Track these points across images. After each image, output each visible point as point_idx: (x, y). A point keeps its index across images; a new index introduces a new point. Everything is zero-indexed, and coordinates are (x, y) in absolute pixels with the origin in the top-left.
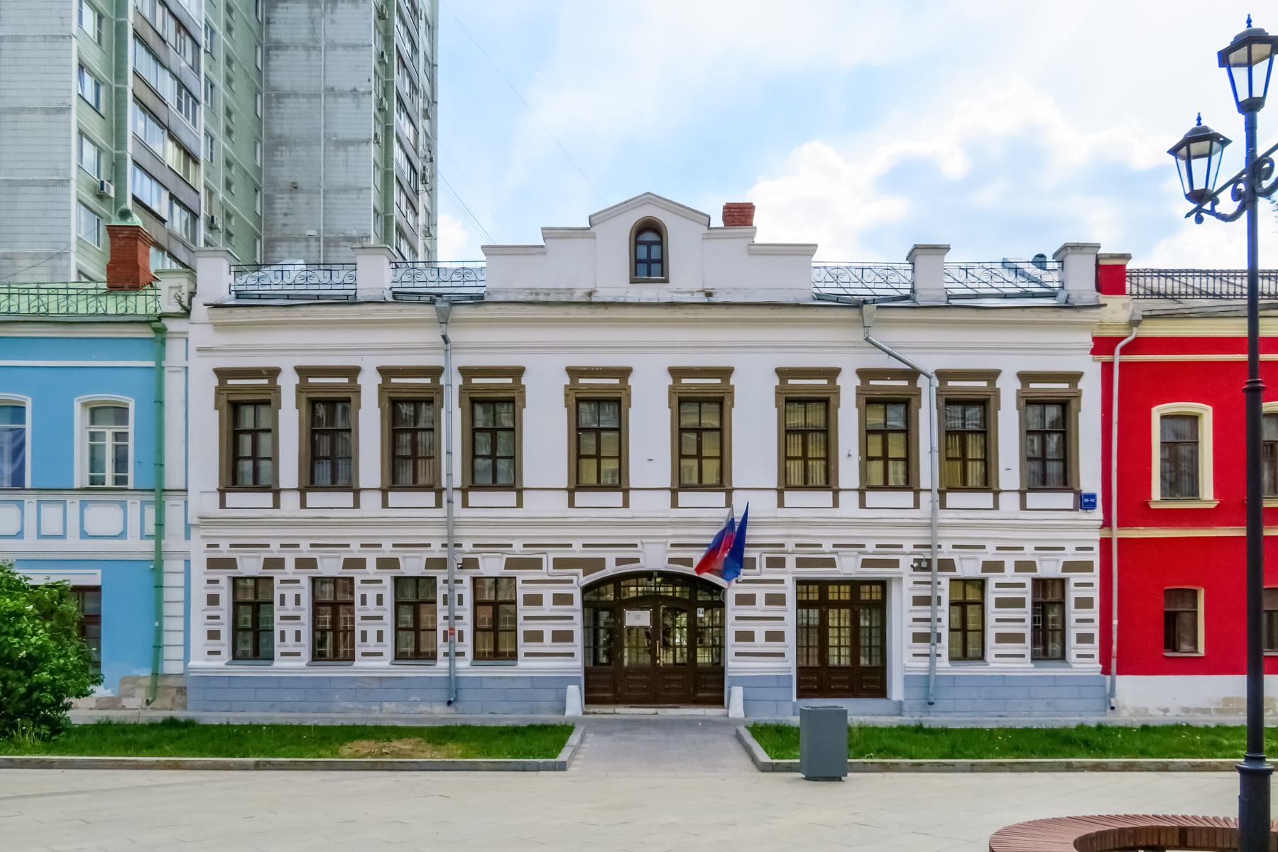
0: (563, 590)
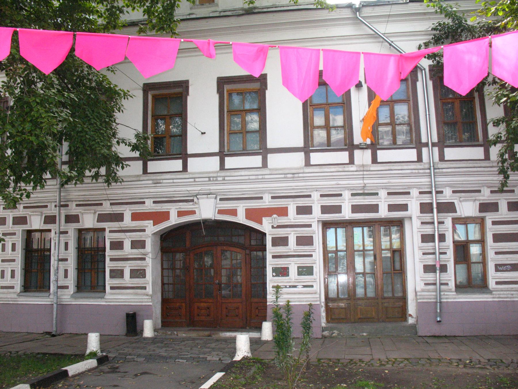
0: (136, 236)
